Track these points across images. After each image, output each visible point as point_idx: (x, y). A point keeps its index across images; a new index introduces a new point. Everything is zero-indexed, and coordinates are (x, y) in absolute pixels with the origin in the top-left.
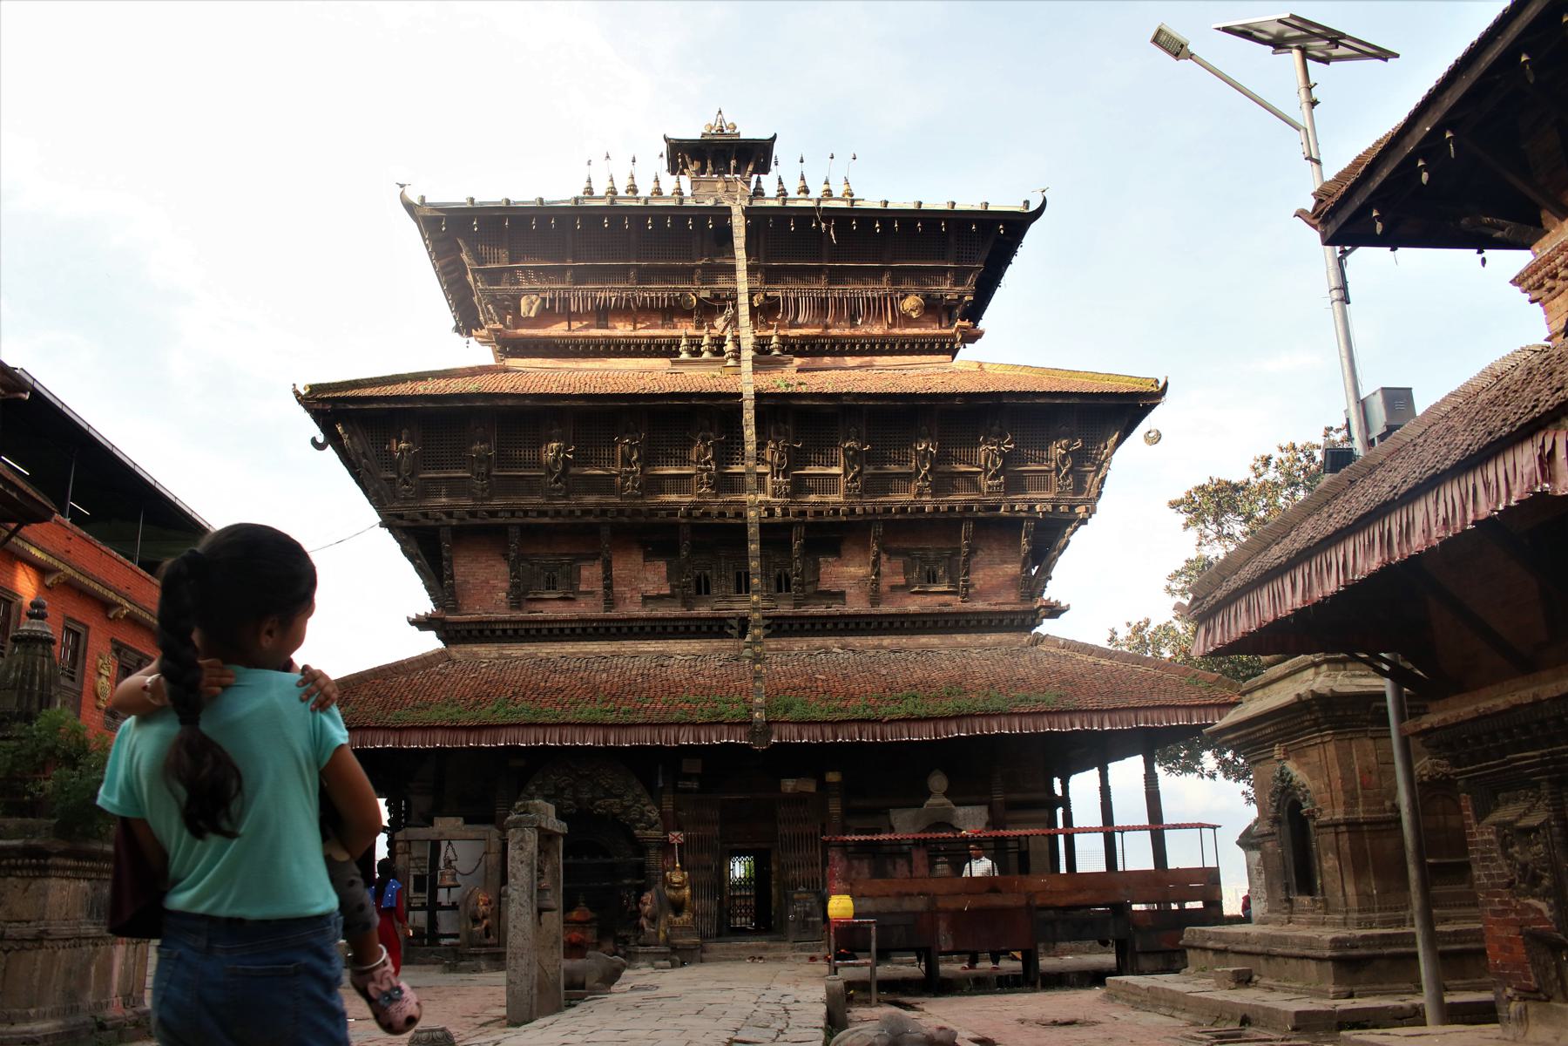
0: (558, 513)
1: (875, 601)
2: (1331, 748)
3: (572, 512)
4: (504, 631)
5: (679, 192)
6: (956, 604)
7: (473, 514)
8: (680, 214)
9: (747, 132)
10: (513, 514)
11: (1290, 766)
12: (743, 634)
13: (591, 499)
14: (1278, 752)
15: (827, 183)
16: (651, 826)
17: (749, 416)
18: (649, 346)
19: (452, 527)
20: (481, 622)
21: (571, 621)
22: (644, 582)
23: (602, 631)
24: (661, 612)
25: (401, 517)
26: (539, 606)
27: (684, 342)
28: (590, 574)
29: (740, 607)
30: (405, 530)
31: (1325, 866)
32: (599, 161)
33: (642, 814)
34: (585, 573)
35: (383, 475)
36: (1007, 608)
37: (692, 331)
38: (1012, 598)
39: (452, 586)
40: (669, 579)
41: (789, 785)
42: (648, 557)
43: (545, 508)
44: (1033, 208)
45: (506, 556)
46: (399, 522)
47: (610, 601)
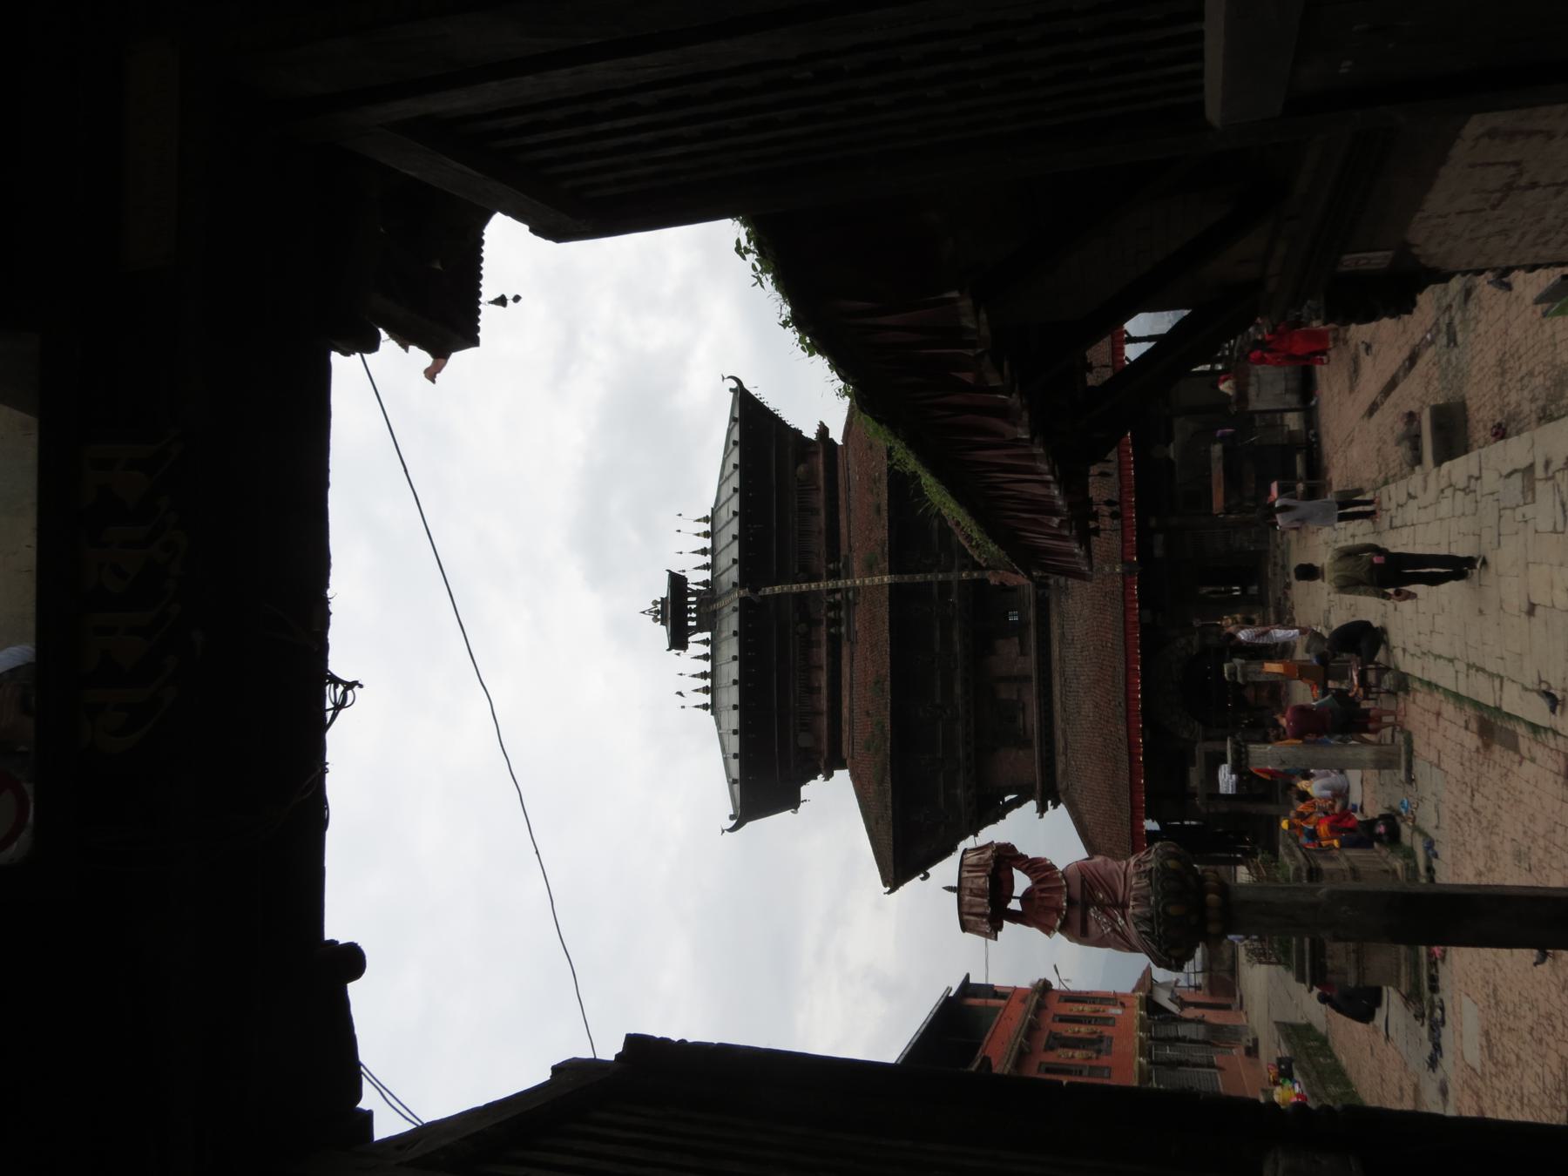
5: (705, 642)
8: (743, 634)
9: (662, 591)
13: (958, 689)
17: (906, 578)
22: (1013, 658)
24: (1033, 643)
37: (823, 628)
41: (1158, 552)
44: (734, 385)
47: (1027, 679)
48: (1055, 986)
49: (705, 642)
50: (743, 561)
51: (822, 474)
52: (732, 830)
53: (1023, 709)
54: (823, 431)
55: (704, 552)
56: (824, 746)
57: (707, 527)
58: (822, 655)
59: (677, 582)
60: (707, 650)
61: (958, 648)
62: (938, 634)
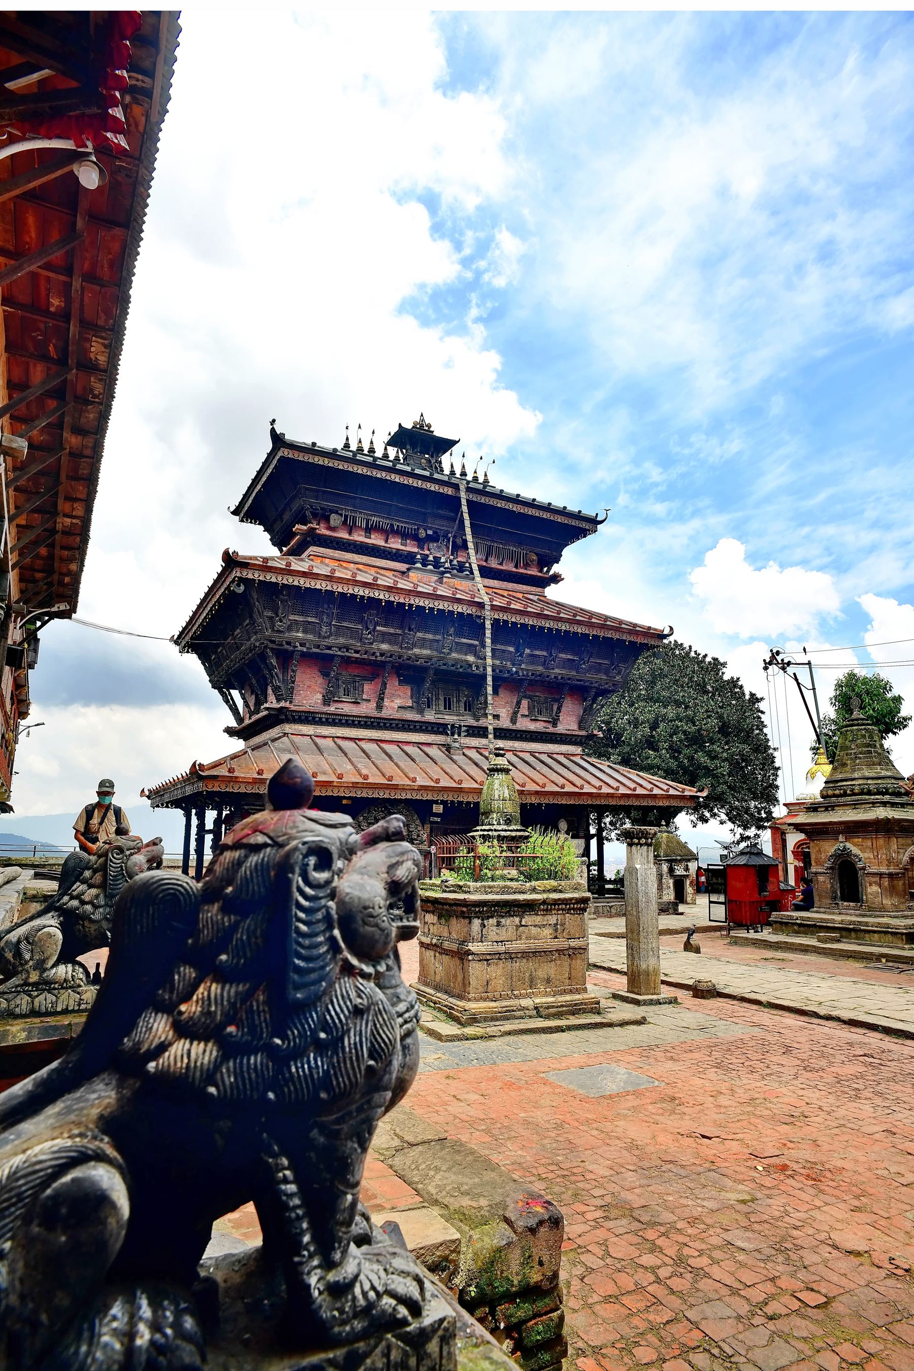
1: (514, 721)
3: (374, 654)
4: (320, 718)
6: (551, 729)
11: (848, 845)
12: (453, 734)
13: (385, 647)
14: (841, 838)
15: (475, 472)
18: (395, 554)
19: (303, 655)
20: (309, 712)
21: (360, 717)
22: (398, 701)
23: (375, 724)
25: (273, 642)
26: (340, 705)
27: (419, 557)
28: (369, 690)
30: (272, 649)
31: (869, 890)
32: (353, 427)
33: (418, 836)
34: (367, 687)
35: (265, 614)
36: (577, 733)
38: (575, 726)
39: (293, 688)
40: (412, 698)
43: (359, 649)
44: (599, 519)
45: (325, 674)
46: (271, 645)
47: (379, 707)
48: (23, 723)
49: (397, 459)
51: (529, 572)
52: (273, 431)
56: (323, 531)
57: (481, 480)
58: (395, 544)
60: (392, 458)
61: (417, 651)
62: (430, 636)
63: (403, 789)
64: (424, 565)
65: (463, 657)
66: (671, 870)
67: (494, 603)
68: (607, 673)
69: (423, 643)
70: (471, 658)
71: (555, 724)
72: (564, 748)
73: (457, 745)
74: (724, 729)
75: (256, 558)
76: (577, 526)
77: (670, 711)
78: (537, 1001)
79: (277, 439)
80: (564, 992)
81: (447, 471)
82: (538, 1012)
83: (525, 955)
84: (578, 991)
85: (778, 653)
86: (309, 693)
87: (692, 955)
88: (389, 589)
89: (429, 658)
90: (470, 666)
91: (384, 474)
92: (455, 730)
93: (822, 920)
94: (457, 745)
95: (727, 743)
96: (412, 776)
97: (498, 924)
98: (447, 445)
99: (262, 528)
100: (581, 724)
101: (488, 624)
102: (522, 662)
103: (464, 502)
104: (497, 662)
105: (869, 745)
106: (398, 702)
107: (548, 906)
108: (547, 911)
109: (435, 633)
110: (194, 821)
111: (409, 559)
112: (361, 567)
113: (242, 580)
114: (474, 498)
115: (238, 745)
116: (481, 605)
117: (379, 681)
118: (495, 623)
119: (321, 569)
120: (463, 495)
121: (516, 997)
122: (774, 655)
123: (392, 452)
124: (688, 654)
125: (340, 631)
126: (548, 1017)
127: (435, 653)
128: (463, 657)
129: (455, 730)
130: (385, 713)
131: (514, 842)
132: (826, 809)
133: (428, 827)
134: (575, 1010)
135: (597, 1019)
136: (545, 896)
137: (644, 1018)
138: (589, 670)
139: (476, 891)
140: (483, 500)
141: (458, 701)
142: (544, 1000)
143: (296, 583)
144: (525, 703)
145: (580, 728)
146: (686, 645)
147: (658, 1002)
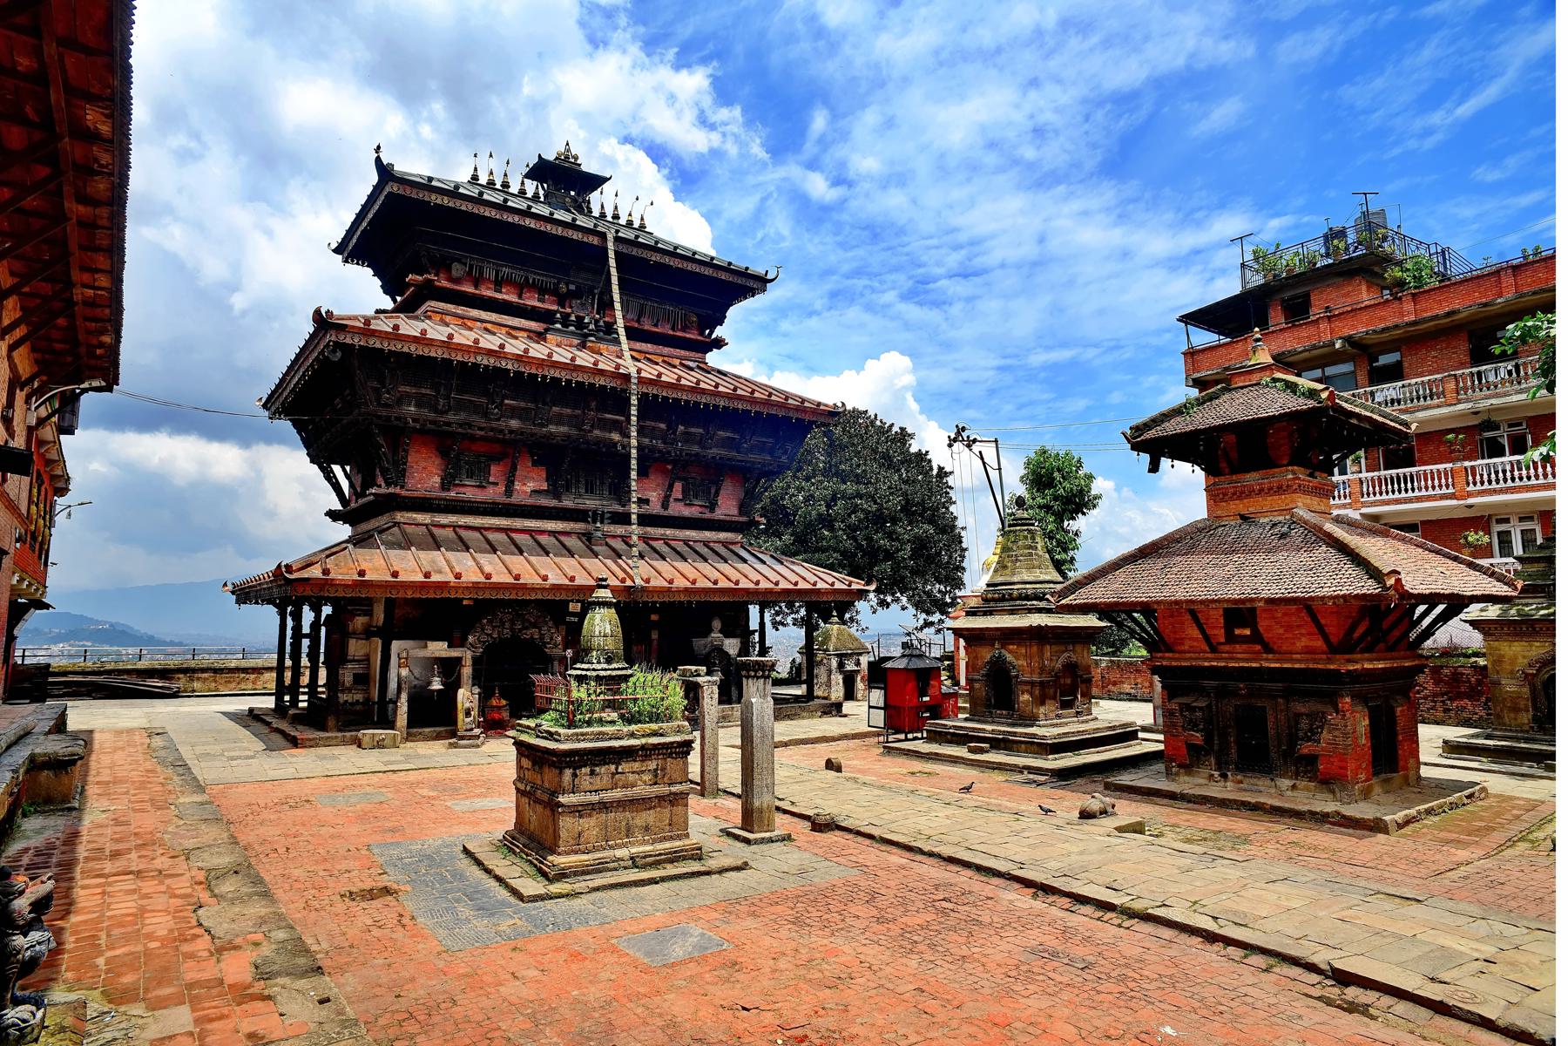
0: (492, 429)
1: (665, 506)
2: (1035, 649)
3: (501, 431)
6: (708, 515)
7: (434, 422)
9: (589, 166)
10: (461, 425)
12: (595, 522)
13: (514, 423)
16: (556, 646)
22: (529, 485)
24: (545, 502)
26: (462, 490)
28: (496, 472)
29: (590, 503)
34: (494, 469)
38: (736, 512)
42: (535, 464)
44: (769, 277)
45: (444, 453)
47: (509, 491)
49: (536, 197)
50: (634, 243)
53: (481, 487)
54: (719, 344)
55: (616, 217)
57: (636, 225)
58: (532, 301)
59: (596, 182)
60: (529, 195)
61: (553, 428)
63: (533, 589)
64: (565, 325)
65: (607, 435)
66: (841, 666)
67: (643, 374)
68: (771, 453)
69: (559, 420)
70: (616, 437)
71: (712, 510)
72: (723, 536)
73: (599, 534)
74: (906, 508)
75: (356, 318)
76: (746, 284)
77: (850, 488)
78: (634, 850)
79: (384, 171)
80: (665, 839)
81: (596, 213)
82: (635, 863)
83: (621, 804)
84: (679, 837)
85: (964, 429)
86: (425, 476)
87: (833, 773)
88: (518, 358)
89: (569, 436)
90: (615, 444)
91: (516, 218)
92: (597, 516)
93: (974, 729)
94: (599, 534)
95: (910, 523)
96: (543, 572)
97: (592, 773)
98: (596, 182)
99: (370, 271)
100: (743, 508)
101: (634, 400)
102: (675, 441)
103: (611, 254)
104: (646, 441)
105: (1030, 547)
106: (531, 486)
107: (646, 752)
108: (647, 757)
109: (574, 408)
110: (290, 623)
111: (545, 317)
112: (489, 326)
113: (338, 345)
114: (624, 249)
115: (343, 531)
116: (627, 377)
117: (508, 461)
118: (643, 398)
119: (437, 332)
120: (610, 245)
121: (611, 847)
122: (960, 430)
123: (531, 187)
124: (872, 423)
125: (460, 406)
126: (644, 867)
127: (574, 432)
128: (607, 435)
129: (597, 516)
130: (515, 499)
131: (614, 682)
132: (985, 614)
133: (563, 628)
134: (674, 857)
135: (695, 866)
136: (643, 741)
137: (746, 864)
138: (751, 450)
139: (568, 739)
140: (635, 252)
141: (602, 483)
142: (641, 849)
143: (406, 350)
144: (678, 486)
145: (741, 514)
146: (871, 413)
147: (771, 840)
